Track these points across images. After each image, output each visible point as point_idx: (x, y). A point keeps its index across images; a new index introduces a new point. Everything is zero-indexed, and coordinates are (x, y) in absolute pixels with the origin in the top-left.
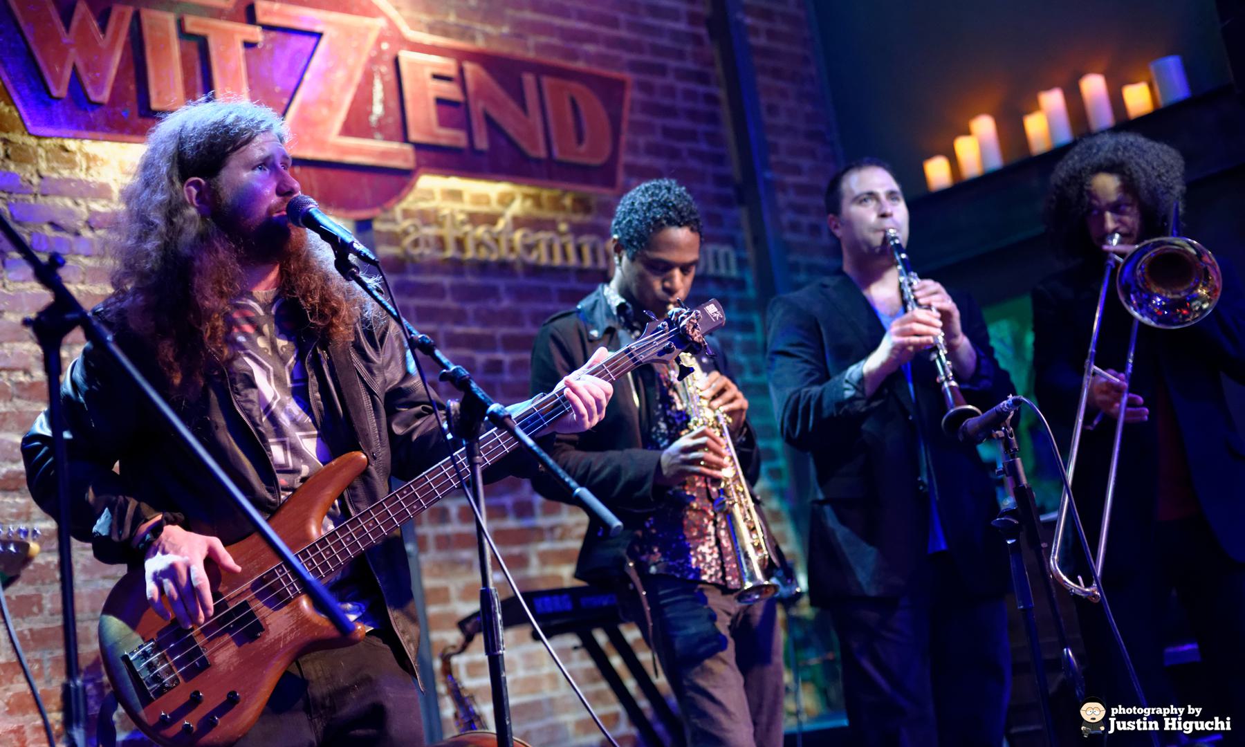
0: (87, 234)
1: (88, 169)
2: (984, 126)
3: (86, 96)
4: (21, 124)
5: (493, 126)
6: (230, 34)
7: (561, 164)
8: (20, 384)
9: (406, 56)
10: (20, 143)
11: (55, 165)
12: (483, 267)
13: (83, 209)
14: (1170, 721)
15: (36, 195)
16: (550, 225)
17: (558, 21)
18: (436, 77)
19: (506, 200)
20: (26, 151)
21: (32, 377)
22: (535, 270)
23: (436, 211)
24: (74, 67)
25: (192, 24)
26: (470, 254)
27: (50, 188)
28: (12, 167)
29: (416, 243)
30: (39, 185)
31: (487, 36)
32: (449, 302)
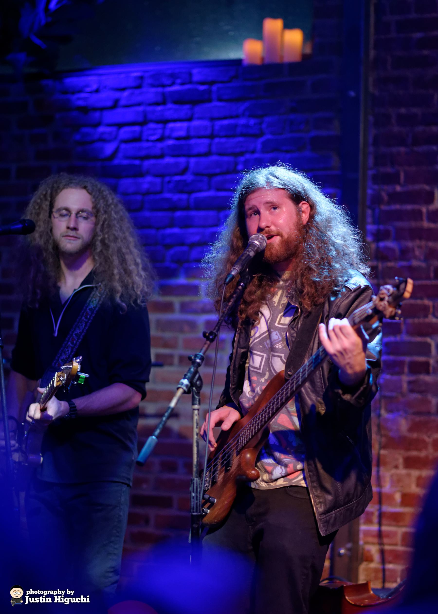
14: (58, 598)
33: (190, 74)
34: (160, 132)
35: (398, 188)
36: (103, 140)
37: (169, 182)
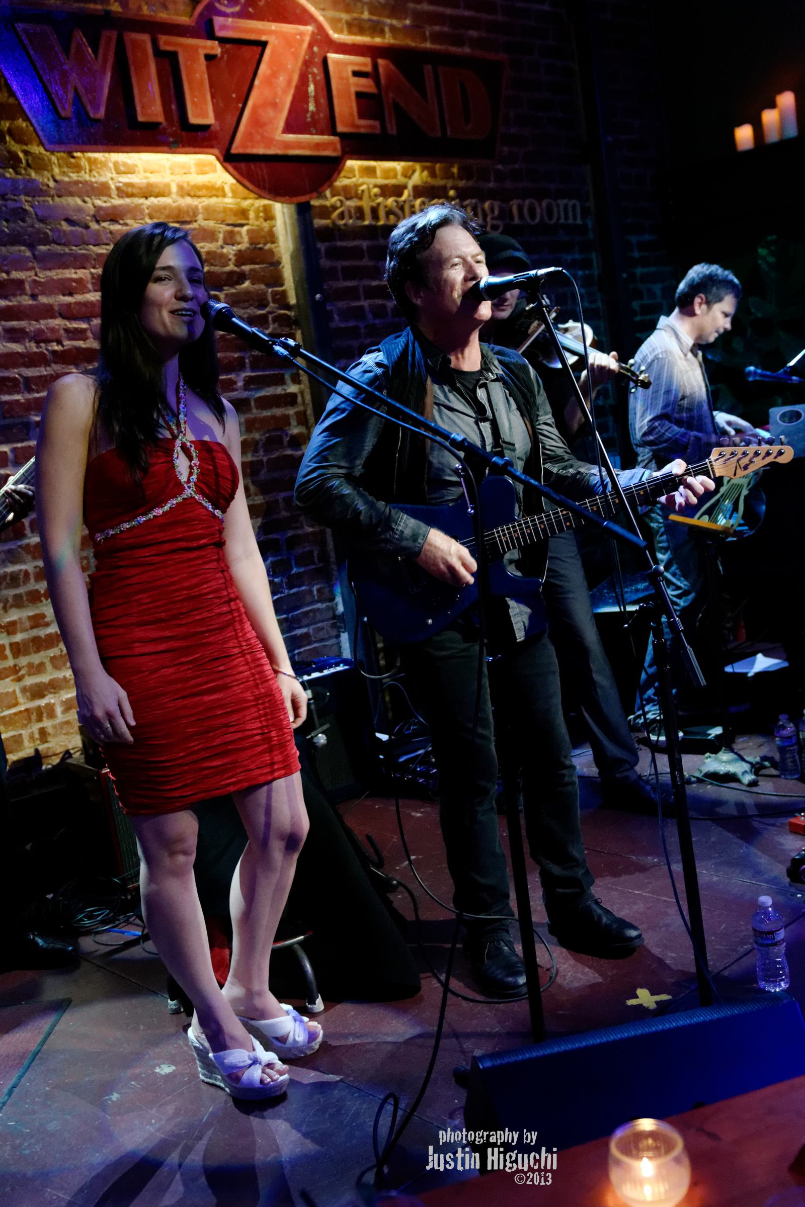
0: (94, 226)
1: (90, 171)
2: (787, 100)
3: (87, 114)
4: (37, 139)
6: (196, 49)
8: (54, 352)
9: (332, 56)
10: (37, 152)
11: (66, 169)
13: (92, 207)
15: (53, 196)
18: (356, 74)
19: (407, 175)
20: (43, 159)
21: (63, 346)
23: (357, 186)
24: (76, 90)
25: (167, 42)
27: (64, 190)
28: (33, 174)
29: (342, 216)
30: (55, 188)
31: (393, 29)
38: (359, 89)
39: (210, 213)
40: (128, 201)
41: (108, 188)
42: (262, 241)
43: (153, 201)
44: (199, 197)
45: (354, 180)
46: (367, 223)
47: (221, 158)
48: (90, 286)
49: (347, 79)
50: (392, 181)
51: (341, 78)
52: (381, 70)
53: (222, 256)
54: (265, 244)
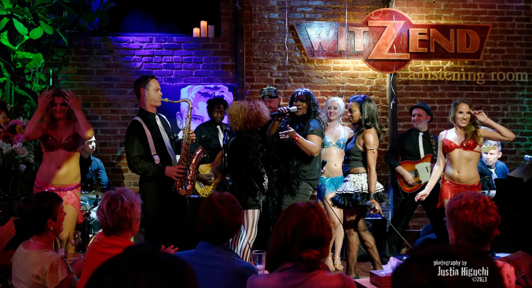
0: (324, 78)
5: (437, 45)
7: (460, 53)
9: (411, 30)
12: (434, 82)
13: (324, 73)
16: (459, 69)
17: (472, 9)
22: (451, 82)
26: (429, 79)
27: (316, 68)
28: (308, 64)
29: (412, 77)
32: (421, 91)
33: (173, 38)
34: (160, 59)
35: (254, 84)
36: (136, 61)
37: (164, 78)
38: (420, 39)
39: (363, 75)
40: (336, 71)
41: (331, 68)
42: (381, 84)
43: (344, 71)
44: (360, 70)
45: (421, 65)
46: (422, 79)
47: (364, 61)
48: (320, 95)
49: (416, 35)
50: (438, 66)
51: (414, 35)
52: (431, 32)
53: (365, 88)
54: (382, 85)
